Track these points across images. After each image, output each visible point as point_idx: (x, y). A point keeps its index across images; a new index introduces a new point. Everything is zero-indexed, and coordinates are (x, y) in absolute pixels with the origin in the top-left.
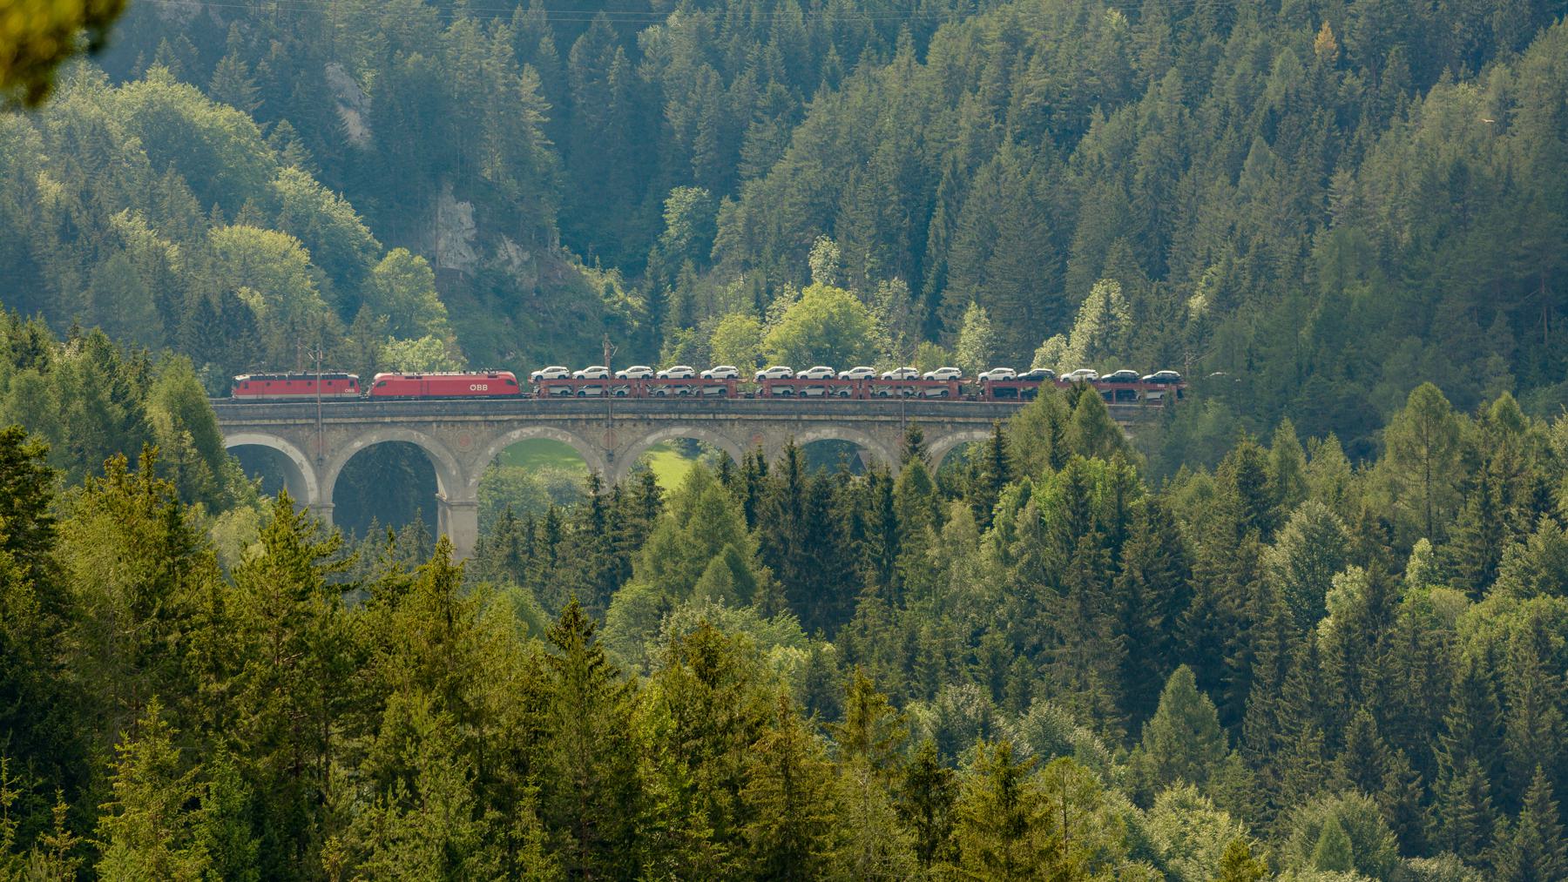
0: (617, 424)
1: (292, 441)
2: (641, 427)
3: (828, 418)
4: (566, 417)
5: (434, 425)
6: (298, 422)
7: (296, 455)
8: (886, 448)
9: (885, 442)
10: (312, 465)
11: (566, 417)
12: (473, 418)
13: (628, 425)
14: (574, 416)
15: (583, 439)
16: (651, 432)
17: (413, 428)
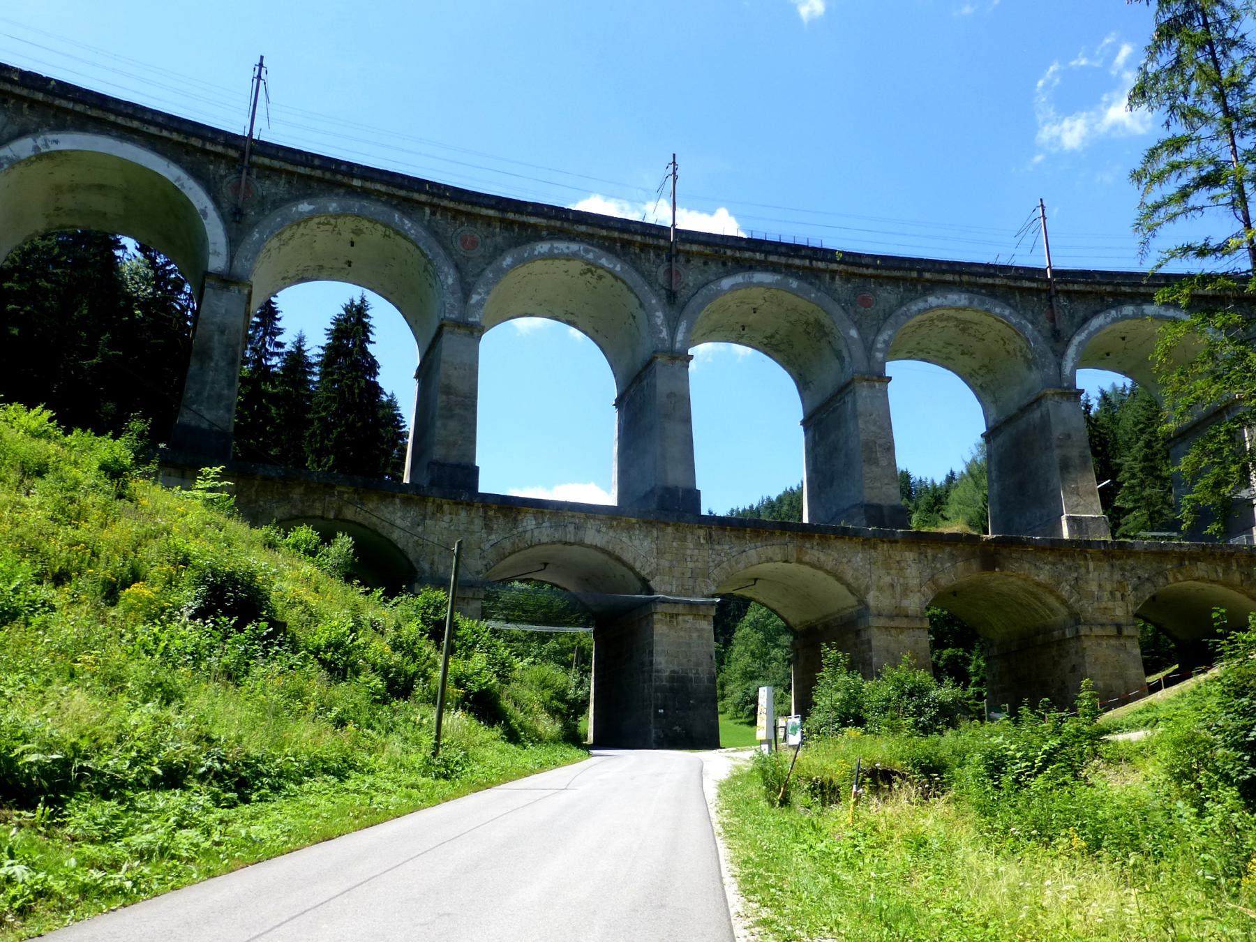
0: (682, 259)
1: (196, 174)
2: (713, 268)
3: (957, 278)
4: (616, 234)
5: (427, 210)
6: (208, 146)
7: (198, 197)
8: (1033, 323)
9: (1029, 315)
10: (223, 217)
11: (616, 234)
12: (484, 212)
13: (696, 262)
14: (626, 236)
15: (637, 270)
16: (728, 274)
17: (395, 207)
